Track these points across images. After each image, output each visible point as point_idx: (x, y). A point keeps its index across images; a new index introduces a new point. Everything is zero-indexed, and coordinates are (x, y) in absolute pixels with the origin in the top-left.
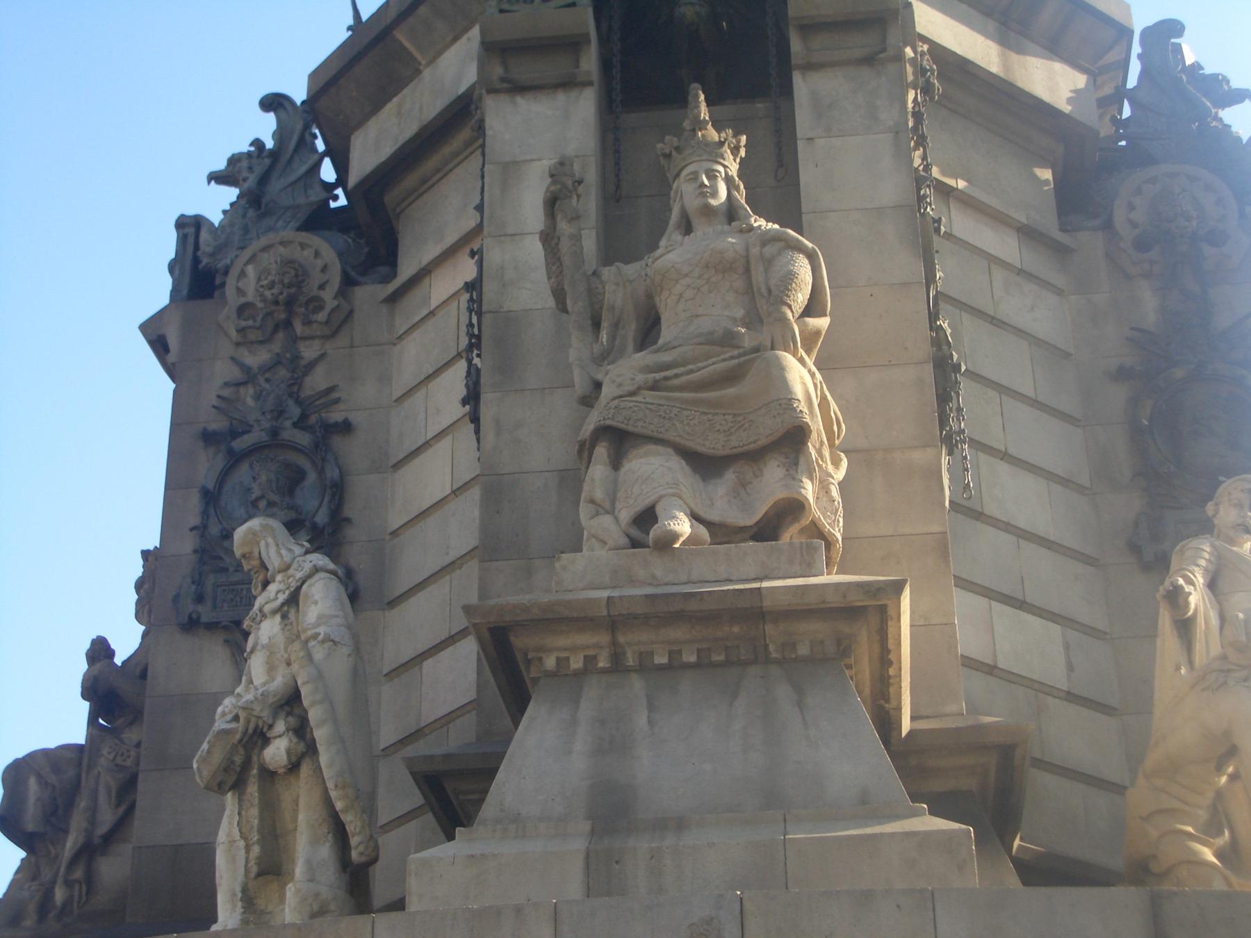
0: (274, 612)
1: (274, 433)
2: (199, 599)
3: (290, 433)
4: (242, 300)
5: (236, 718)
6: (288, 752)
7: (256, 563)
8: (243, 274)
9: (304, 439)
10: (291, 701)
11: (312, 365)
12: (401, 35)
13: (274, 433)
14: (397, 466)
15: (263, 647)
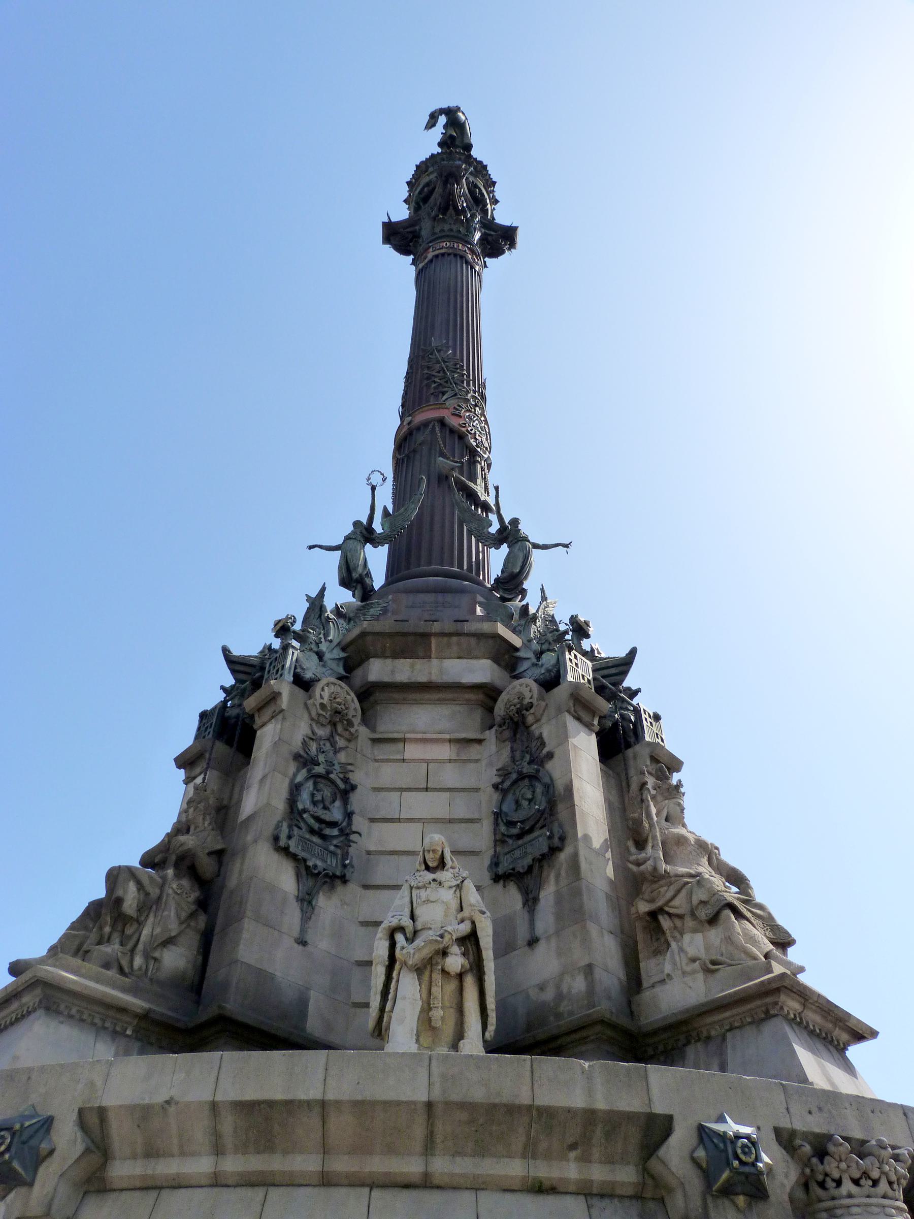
0: (451, 887)
1: (328, 772)
2: (289, 837)
3: (332, 776)
4: (322, 701)
5: (442, 936)
6: (462, 966)
7: (438, 856)
8: (323, 689)
9: (342, 785)
10: (470, 940)
11: (341, 749)
12: (434, 641)
13: (328, 772)
14: (372, 820)
15: (443, 902)
